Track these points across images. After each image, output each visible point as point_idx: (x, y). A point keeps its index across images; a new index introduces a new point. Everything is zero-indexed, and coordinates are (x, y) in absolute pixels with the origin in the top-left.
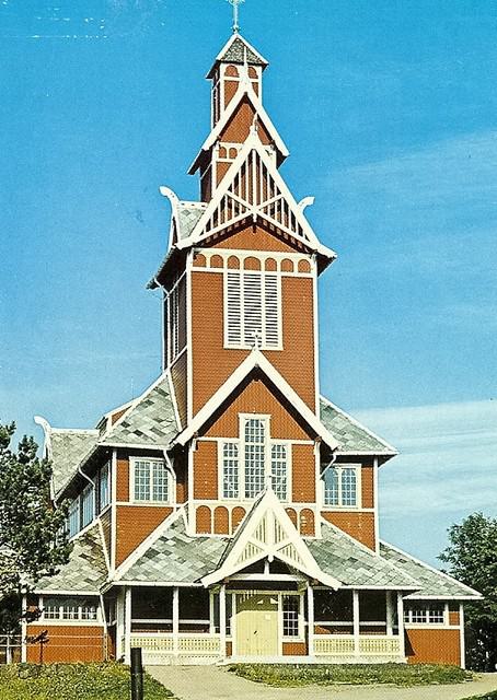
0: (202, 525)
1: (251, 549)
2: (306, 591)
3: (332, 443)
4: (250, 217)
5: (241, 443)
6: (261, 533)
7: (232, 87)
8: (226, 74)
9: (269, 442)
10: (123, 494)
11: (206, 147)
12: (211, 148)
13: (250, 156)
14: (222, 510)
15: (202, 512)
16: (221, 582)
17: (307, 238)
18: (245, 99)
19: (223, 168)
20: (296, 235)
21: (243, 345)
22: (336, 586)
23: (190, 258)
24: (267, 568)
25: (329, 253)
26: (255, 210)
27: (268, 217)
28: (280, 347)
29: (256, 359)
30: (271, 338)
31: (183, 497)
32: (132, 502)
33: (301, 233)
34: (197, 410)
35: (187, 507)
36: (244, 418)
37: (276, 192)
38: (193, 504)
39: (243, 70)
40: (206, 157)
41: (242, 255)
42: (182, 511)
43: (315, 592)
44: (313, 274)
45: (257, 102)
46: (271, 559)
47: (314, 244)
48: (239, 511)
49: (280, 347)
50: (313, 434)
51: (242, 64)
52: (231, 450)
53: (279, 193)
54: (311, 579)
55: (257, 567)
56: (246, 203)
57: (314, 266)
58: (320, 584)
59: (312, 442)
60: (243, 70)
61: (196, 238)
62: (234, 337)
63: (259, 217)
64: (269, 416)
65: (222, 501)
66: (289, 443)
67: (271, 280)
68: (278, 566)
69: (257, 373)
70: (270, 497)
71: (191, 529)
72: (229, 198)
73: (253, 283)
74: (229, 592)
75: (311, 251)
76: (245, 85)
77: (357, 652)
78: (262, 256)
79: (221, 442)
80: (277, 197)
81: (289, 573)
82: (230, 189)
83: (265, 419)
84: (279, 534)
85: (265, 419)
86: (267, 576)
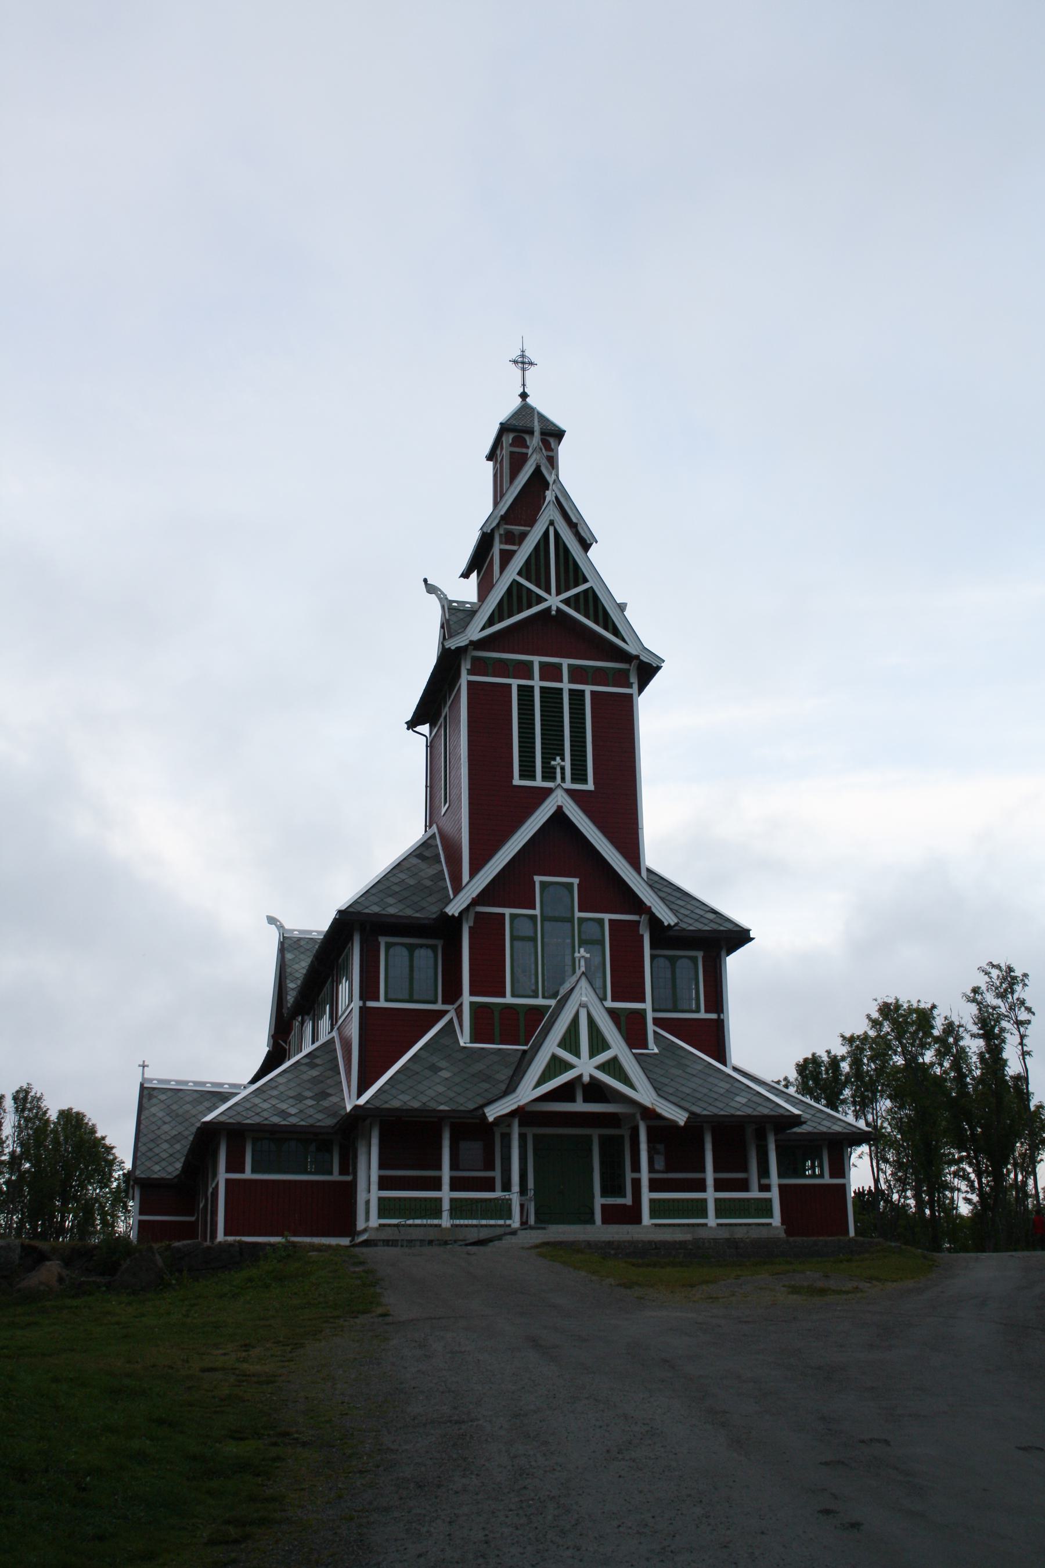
1: (557, 1065)
2: (635, 1132)
3: (667, 918)
4: (549, 609)
6: (570, 1041)
8: (511, 445)
10: (368, 990)
13: (546, 534)
16: (512, 1114)
17: (624, 640)
21: (539, 782)
22: (680, 1117)
23: (465, 666)
24: (579, 1097)
26: (554, 601)
28: (590, 786)
30: (579, 775)
31: (452, 994)
32: (382, 1004)
34: (475, 869)
35: (459, 1012)
37: (581, 580)
38: (467, 999)
42: (452, 1014)
43: (650, 1131)
46: (586, 1079)
49: (590, 786)
50: (636, 905)
53: (586, 580)
55: (565, 1093)
57: (634, 679)
58: (660, 1117)
62: (528, 772)
63: (558, 610)
64: (576, 881)
65: (509, 999)
66: (607, 917)
67: (577, 697)
68: (595, 1091)
71: (464, 1040)
73: (552, 697)
74: (525, 1130)
77: (712, 1221)
78: (565, 663)
81: (615, 1102)
84: (598, 1043)
86: (580, 1106)
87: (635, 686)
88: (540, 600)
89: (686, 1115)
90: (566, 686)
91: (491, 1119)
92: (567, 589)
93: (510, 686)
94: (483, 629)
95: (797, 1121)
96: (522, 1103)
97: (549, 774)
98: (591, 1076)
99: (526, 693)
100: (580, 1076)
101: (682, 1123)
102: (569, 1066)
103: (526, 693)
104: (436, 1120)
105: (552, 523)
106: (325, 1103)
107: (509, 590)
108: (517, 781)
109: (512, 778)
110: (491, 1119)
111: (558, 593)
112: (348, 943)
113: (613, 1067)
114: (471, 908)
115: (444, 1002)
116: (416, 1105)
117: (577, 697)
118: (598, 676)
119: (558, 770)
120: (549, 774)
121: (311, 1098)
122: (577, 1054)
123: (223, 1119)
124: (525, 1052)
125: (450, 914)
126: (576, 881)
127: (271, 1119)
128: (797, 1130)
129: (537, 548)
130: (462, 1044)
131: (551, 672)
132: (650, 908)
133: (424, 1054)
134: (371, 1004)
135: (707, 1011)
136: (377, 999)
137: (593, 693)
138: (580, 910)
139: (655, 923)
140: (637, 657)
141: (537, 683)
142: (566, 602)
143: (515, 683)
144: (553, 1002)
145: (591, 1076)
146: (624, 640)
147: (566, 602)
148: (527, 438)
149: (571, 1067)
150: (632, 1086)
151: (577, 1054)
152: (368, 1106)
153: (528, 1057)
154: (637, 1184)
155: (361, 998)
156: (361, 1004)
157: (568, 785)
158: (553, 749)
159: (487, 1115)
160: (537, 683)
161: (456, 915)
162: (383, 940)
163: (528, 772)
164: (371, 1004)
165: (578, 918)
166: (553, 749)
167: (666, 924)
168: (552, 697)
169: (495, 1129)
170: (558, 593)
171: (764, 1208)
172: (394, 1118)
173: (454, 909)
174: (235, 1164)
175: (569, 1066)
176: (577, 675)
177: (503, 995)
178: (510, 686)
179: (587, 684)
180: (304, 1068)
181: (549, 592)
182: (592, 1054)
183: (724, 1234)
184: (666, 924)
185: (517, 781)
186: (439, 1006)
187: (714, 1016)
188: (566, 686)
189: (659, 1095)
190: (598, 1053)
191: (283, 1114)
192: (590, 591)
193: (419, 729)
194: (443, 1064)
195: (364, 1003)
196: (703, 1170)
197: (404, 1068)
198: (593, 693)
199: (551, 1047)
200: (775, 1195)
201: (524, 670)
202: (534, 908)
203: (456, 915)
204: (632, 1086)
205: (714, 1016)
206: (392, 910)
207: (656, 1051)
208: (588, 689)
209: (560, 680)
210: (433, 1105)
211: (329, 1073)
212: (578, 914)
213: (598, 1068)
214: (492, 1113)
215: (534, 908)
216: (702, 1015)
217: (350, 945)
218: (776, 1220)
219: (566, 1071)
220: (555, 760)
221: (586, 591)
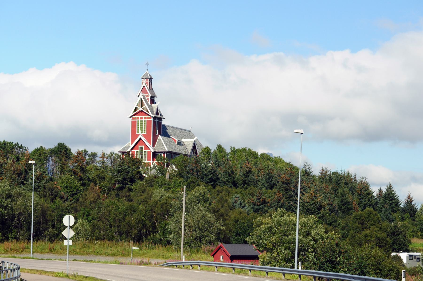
5: (139, 151)
9: (144, 151)
26: (141, 109)
27: (143, 110)
28: (146, 133)
29: (140, 136)
30: (144, 132)
33: (149, 112)
36: (139, 146)
41: (140, 117)
49: (146, 133)
56: (139, 108)
62: (138, 132)
67: (145, 121)
69: (140, 139)
73: (141, 121)
78: (143, 117)
79: (136, 151)
80: (145, 106)
83: (143, 146)
85: (143, 146)
99: (138, 121)
109: (136, 133)
118: (148, 118)
143: (137, 120)
157: (143, 133)
160: (140, 120)
166: (141, 130)
168: (141, 121)
176: (145, 118)
179: (146, 119)
185: (137, 134)
201: (138, 118)
208: (146, 120)
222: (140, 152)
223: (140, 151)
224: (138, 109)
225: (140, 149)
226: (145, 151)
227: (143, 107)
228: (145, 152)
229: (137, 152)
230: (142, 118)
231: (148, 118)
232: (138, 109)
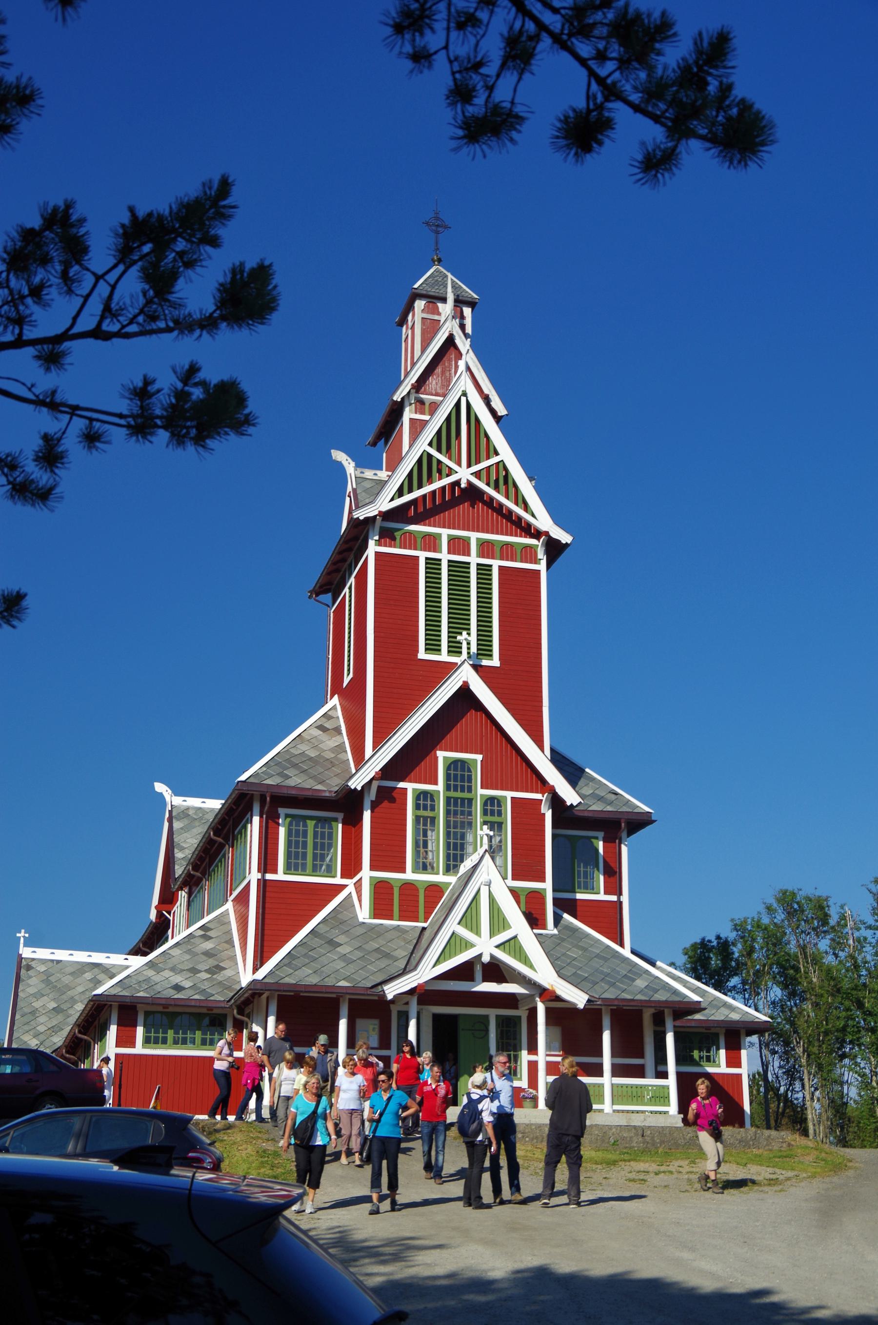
0: (381, 908)
1: (455, 944)
2: (533, 1012)
3: (570, 796)
4: (457, 483)
7: (431, 328)
10: (267, 863)
11: (397, 397)
12: (403, 399)
13: (458, 405)
14: (409, 888)
15: (381, 890)
16: (412, 992)
17: (533, 515)
18: (450, 341)
19: (417, 427)
20: (519, 511)
21: (444, 657)
22: (578, 998)
25: (565, 538)
26: (464, 474)
28: (495, 662)
31: (351, 868)
32: (280, 876)
33: (526, 507)
34: (379, 740)
35: (358, 886)
38: (366, 874)
39: (446, 309)
40: (397, 410)
41: (445, 533)
42: (351, 889)
43: (549, 1011)
44: (542, 567)
45: (463, 345)
46: (486, 959)
47: (543, 521)
48: (435, 891)
49: (495, 662)
51: (444, 300)
52: (425, 800)
53: (497, 453)
54: (545, 993)
55: (465, 971)
57: (541, 554)
58: (558, 999)
59: (538, 796)
60: (446, 309)
61: (385, 503)
62: (433, 646)
63: (469, 482)
64: (479, 757)
65: (409, 875)
66: (509, 795)
67: (484, 571)
70: (489, 871)
71: (363, 913)
72: (430, 456)
73: (459, 570)
75: (537, 534)
76: (450, 327)
78: (474, 537)
79: (410, 787)
82: (430, 444)
84: (498, 922)
87: (544, 563)
88: (451, 472)
89: (586, 997)
90: (474, 560)
91: (390, 997)
92: (478, 461)
93: (417, 558)
94: (392, 499)
95: (696, 1008)
96: (422, 981)
97: (455, 648)
98: (492, 956)
99: (433, 565)
100: (480, 955)
101: (581, 1005)
102: (468, 945)
103: (433, 565)
104: (334, 996)
105: (464, 394)
106: (220, 977)
107: (420, 461)
108: (422, 655)
109: (418, 651)
110: (390, 997)
111: (469, 465)
112: (247, 814)
113: (512, 945)
114: (374, 782)
115: (342, 877)
116: (314, 980)
117: (484, 571)
118: (507, 551)
119: (464, 645)
120: (455, 648)
121: (206, 971)
122: (478, 933)
123: (114, 992)
124: (424, 929)
125: (353, 787)
126: (479, 757)
127: (164, 992)
128: (698, 1016)
129: (448, 419)
130: (361, 920)
131: (459, 545)
132: (553, 787)
133: (323, 929)
134: (269, 876)
135: (606, 893)
136: (275, 871)
137: (501, 568)
138: (482, 788)
139: (557, 802)
140: (547, 534)
141: (444, 556)
142: (477, 474)
143: (422, 555)
144: (452, 879)
145: (492, 956)
146: (533, 515)
147: (477, 474)
148: (440, 305)
149: (472, 946)
150: (531, 966)
151: (478, 933)
152: (266, 980)
153: (427, 934)
154: (533, 1066)
155: (259, 871)
156: (259, 876)
158: (459, 623)
159: (386, 992)
160: (444, 556)
161: (359, 788)
162: (282, 811)
163: (433, 646)
164: (269, 876)
165: (481, 795)
166: (459, 623)
167: (568, 804)
168: (459, 570)
169: (392, 1006)
170: (469, 465)
171: (661, 1097)
172: (292, 994)
173: (356, 783)
174: (125, 1040)
175: (468, 945)
176: (486, 549)
177: (403, 870)
178: (417, 558)
179: (493, 558)
180: (197, 941)
181: (459, 463)
182: (492, 934)
183: (622, 1121)
184: (568, 804)
185: (422, 655)
186: (338, 880)
187: (614, 898)
188: (474, 560)
189: (560, 975)
190: (499, 932)
191: (178, 988)
192: (501, 465)
193: (322, 597)
194: (341, 939)
195: (263, 876)
196: (600, 1054)
197: (301, 944)
198: (501, 568)
199: (452, 925)
200: (671, 1082)
201: (431, 543)
202: (436, 783)
203: (359, 788)
204: (531, 966)
205: (614, 898)
206: (291, 782)
207: (555, 932)
208: (496, 564)
209: (469, 555)
210: (330, 982)
211: (226, 946)
212: (482, 792)
213: (497, 947)
214: (391, 991)
215: (436, 783)
216: (602, 897)
217: (249, 815)
218: (673, 1107)
219: (467, 948)
220: (461, 634)
221: (497, 464)
222: (448, 800)
223: (452, 794)
224: (442, 470)
225: (448, 777)
226: (491, 800)
227: (475, 468)
228: (492, 805)
229: (425, 800)
230: (459, 545)
231: (507, 551)
232: (442, 470)
